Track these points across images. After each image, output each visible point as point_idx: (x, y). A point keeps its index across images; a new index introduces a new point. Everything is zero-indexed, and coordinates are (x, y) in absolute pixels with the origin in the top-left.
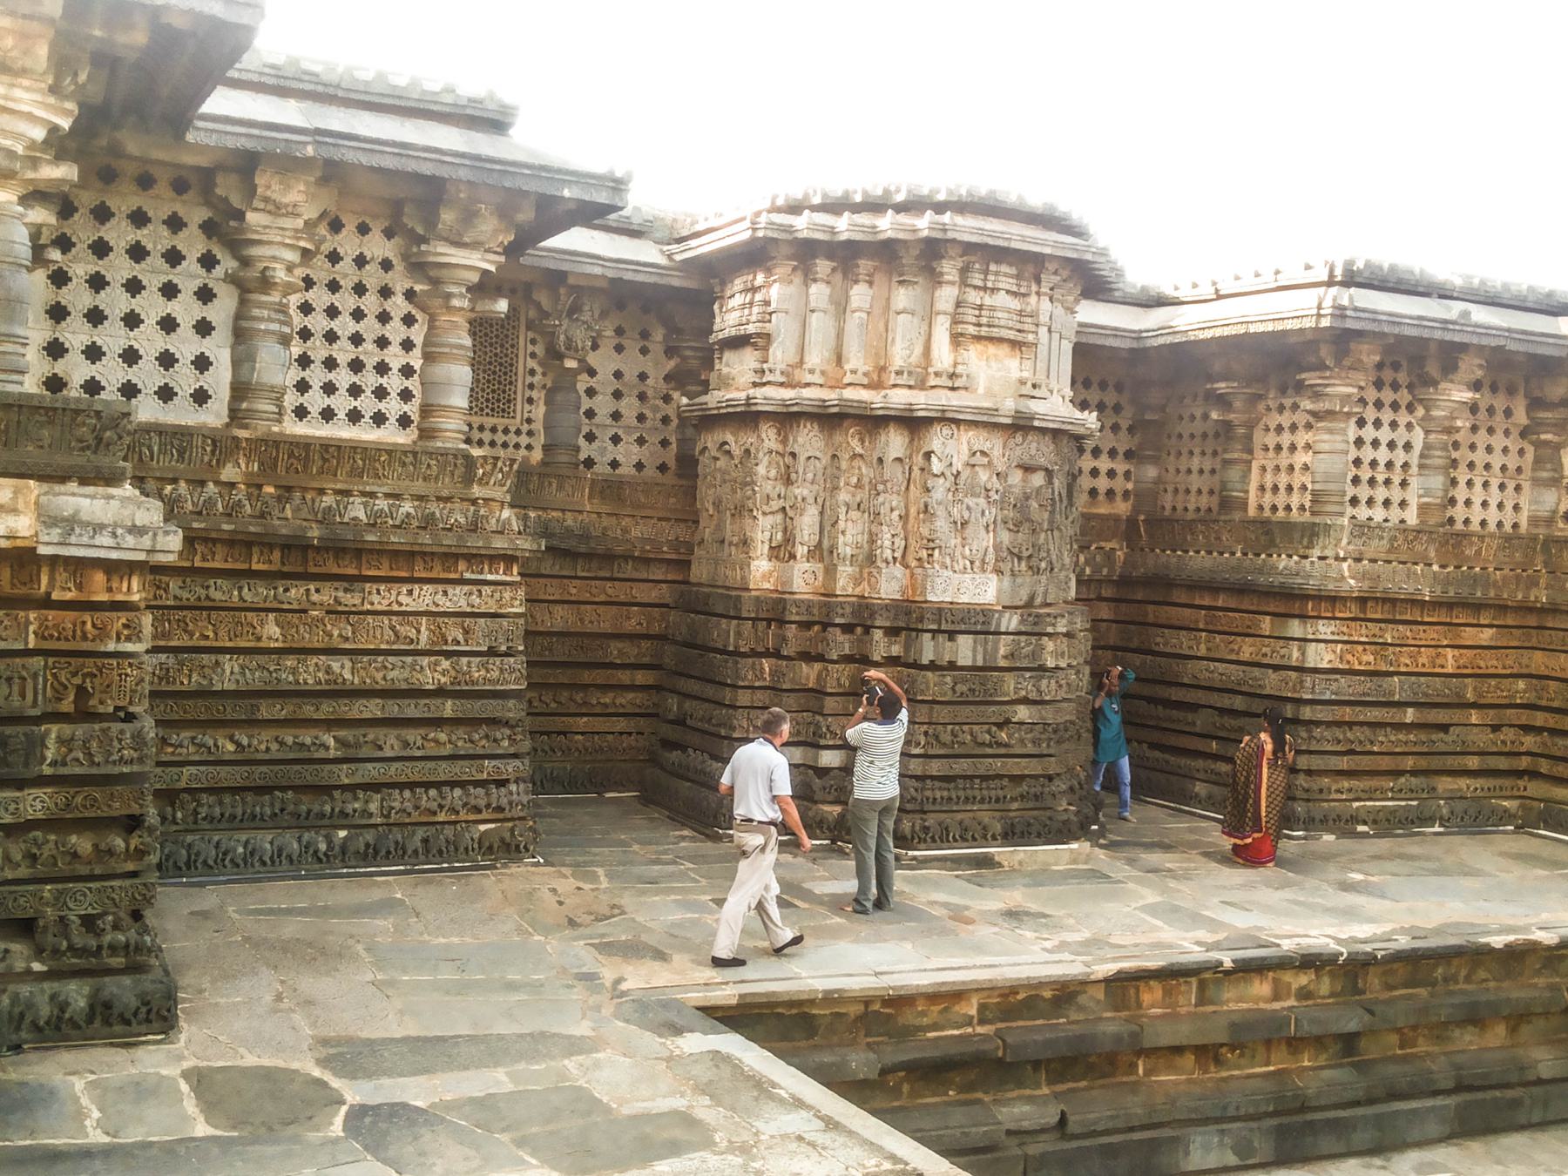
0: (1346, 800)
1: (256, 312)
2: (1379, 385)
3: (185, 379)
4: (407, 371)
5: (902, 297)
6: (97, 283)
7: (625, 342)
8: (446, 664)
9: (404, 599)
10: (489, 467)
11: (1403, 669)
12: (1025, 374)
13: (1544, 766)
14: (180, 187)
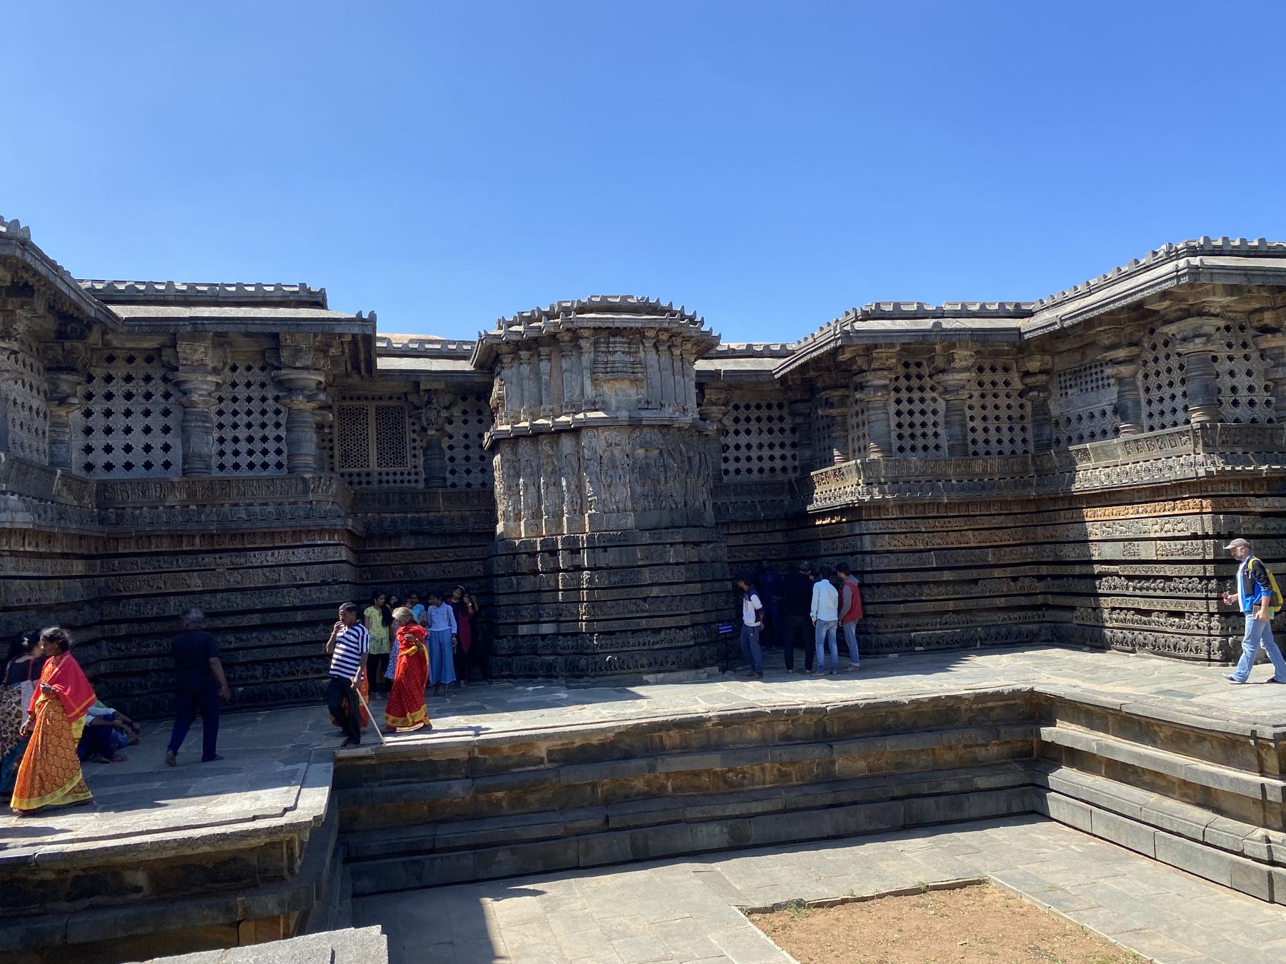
0: (905, 632)
1: (189, 417)
2: (908, 377)
3: (157, 457)
4: (278, 439)
5: (565, 364)
6: (108, 413)
7: (468, 418)
8: (294, 591)
9: (270, 558)
10: (317, 483)
11: (935, 547)
12: (640, 396)
13: (1051, 600)
14: (149, 360)
